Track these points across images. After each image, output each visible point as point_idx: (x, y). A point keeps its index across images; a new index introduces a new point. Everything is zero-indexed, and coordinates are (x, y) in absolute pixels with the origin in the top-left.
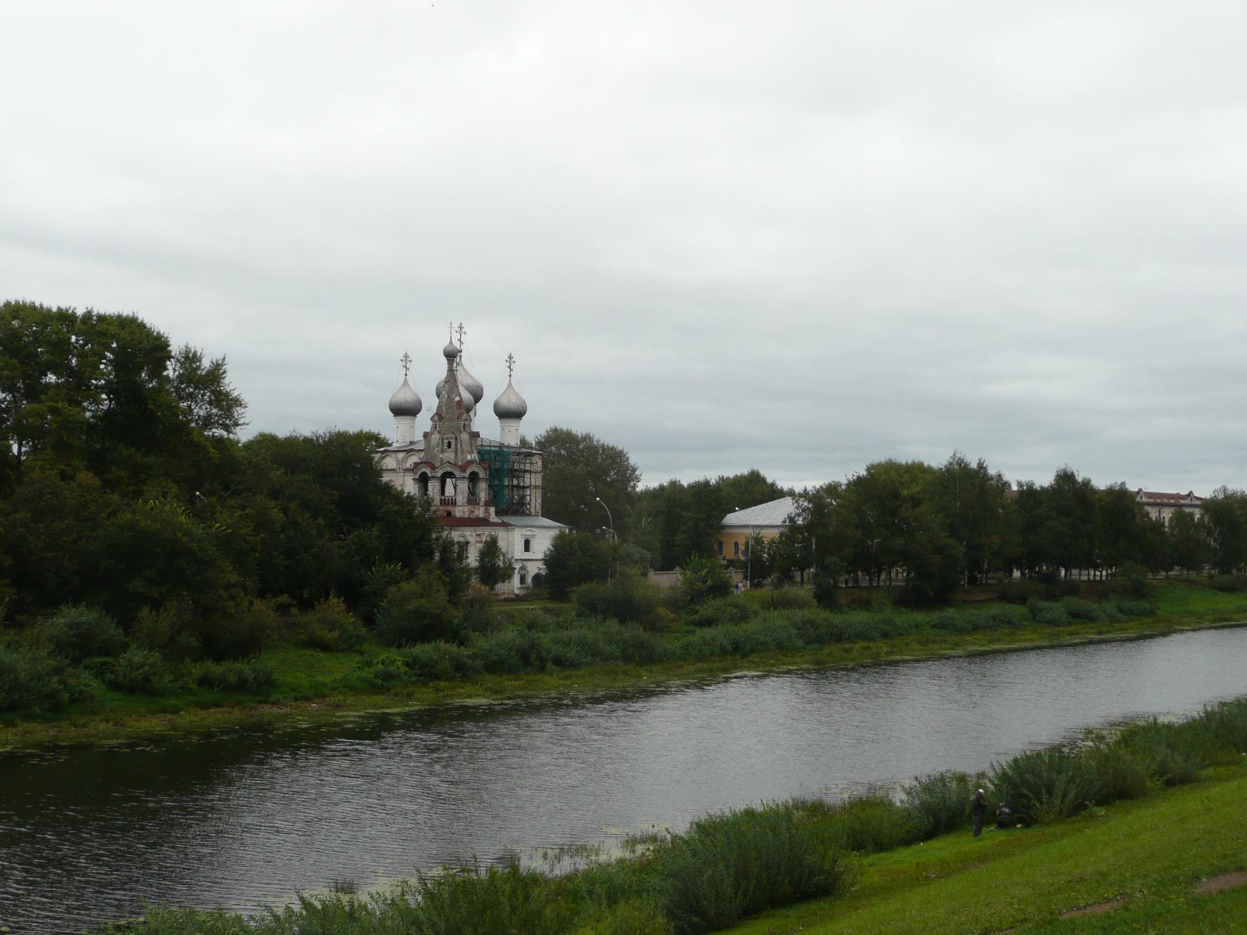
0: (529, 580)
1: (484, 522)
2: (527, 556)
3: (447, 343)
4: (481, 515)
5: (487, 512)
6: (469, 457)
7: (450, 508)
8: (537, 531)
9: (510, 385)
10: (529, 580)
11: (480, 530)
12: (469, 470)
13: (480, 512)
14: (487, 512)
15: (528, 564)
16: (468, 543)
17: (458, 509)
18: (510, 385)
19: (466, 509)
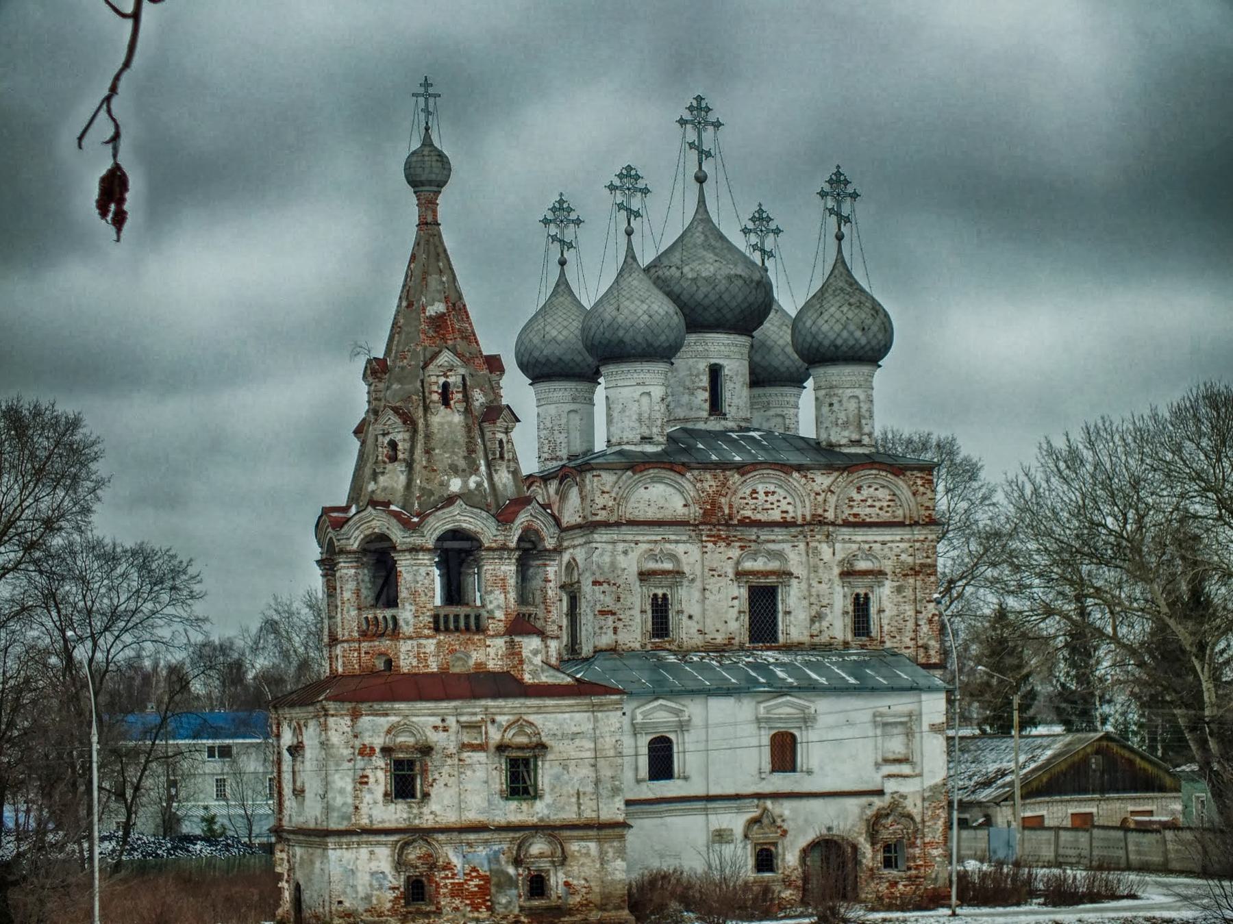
0: (790, 858)
1: (504, 685)
2: (781, 783)
3: (416, 145)
4: (493, 665)
5: (513, 651)
6: (455, 485)
7: (385, 644)
8: (822, 706)
9: (840, 260)
10: (790, 858)
11: (475, 710)
12: (438, 524)
13: (490, 653)
14: (513, 651)
15: (785, 809)
16: (427, 750)
17: (405, 646)
18: (840, 260)
19: (430, 645)
